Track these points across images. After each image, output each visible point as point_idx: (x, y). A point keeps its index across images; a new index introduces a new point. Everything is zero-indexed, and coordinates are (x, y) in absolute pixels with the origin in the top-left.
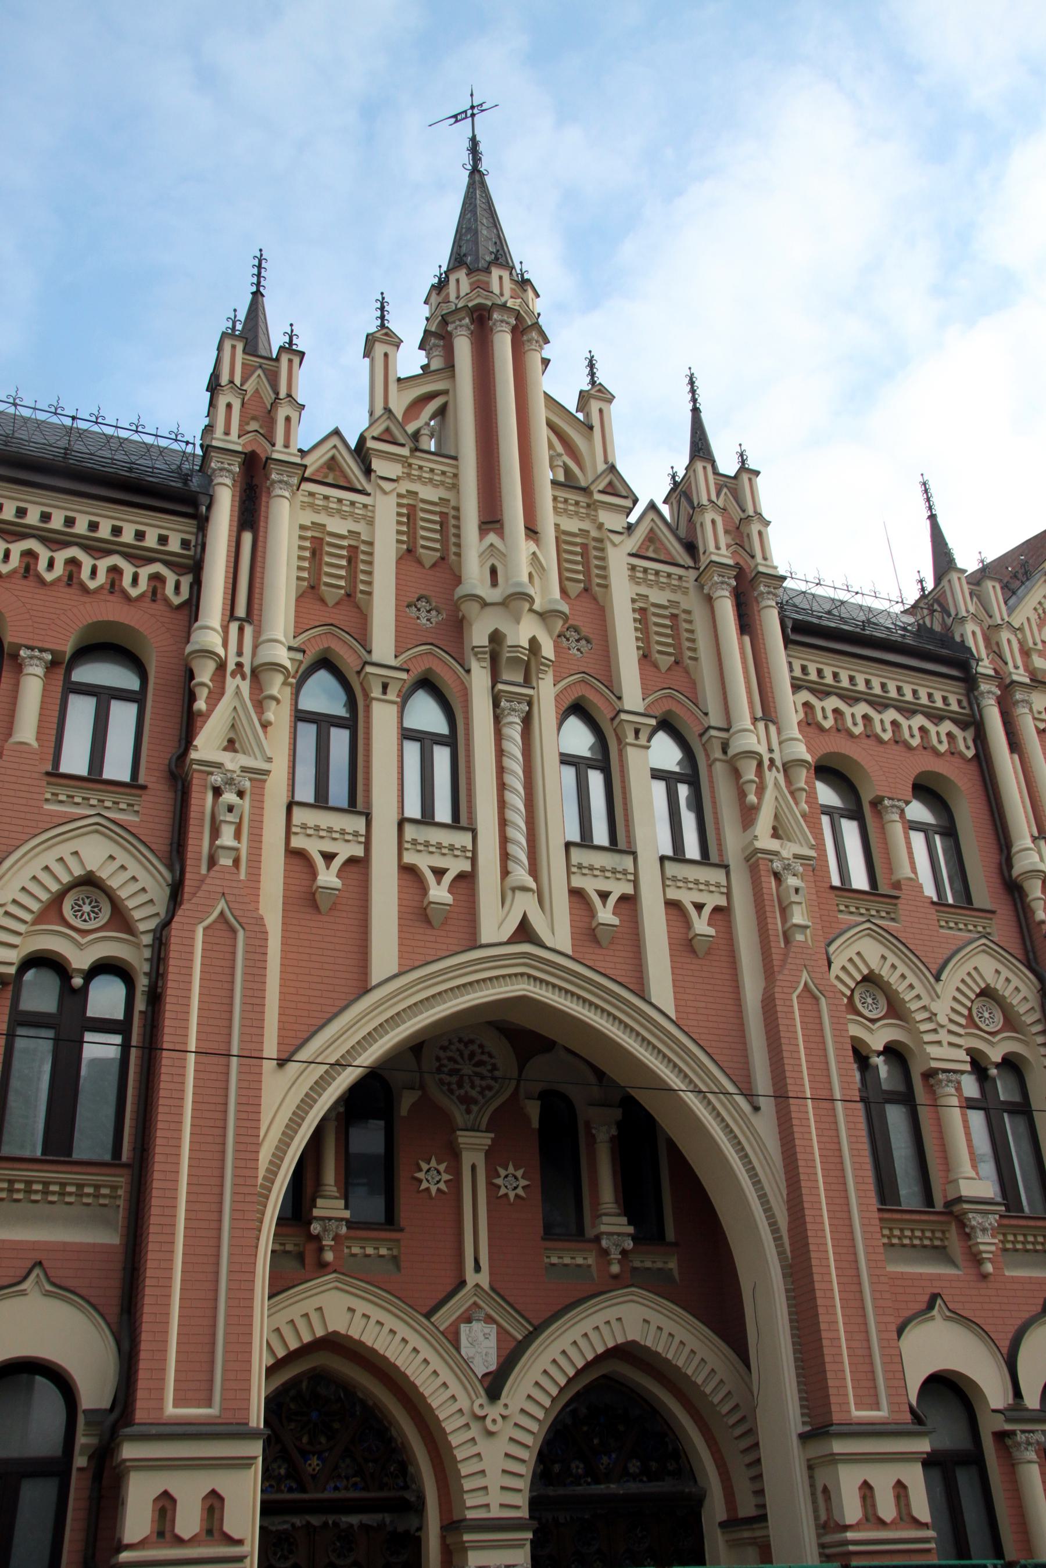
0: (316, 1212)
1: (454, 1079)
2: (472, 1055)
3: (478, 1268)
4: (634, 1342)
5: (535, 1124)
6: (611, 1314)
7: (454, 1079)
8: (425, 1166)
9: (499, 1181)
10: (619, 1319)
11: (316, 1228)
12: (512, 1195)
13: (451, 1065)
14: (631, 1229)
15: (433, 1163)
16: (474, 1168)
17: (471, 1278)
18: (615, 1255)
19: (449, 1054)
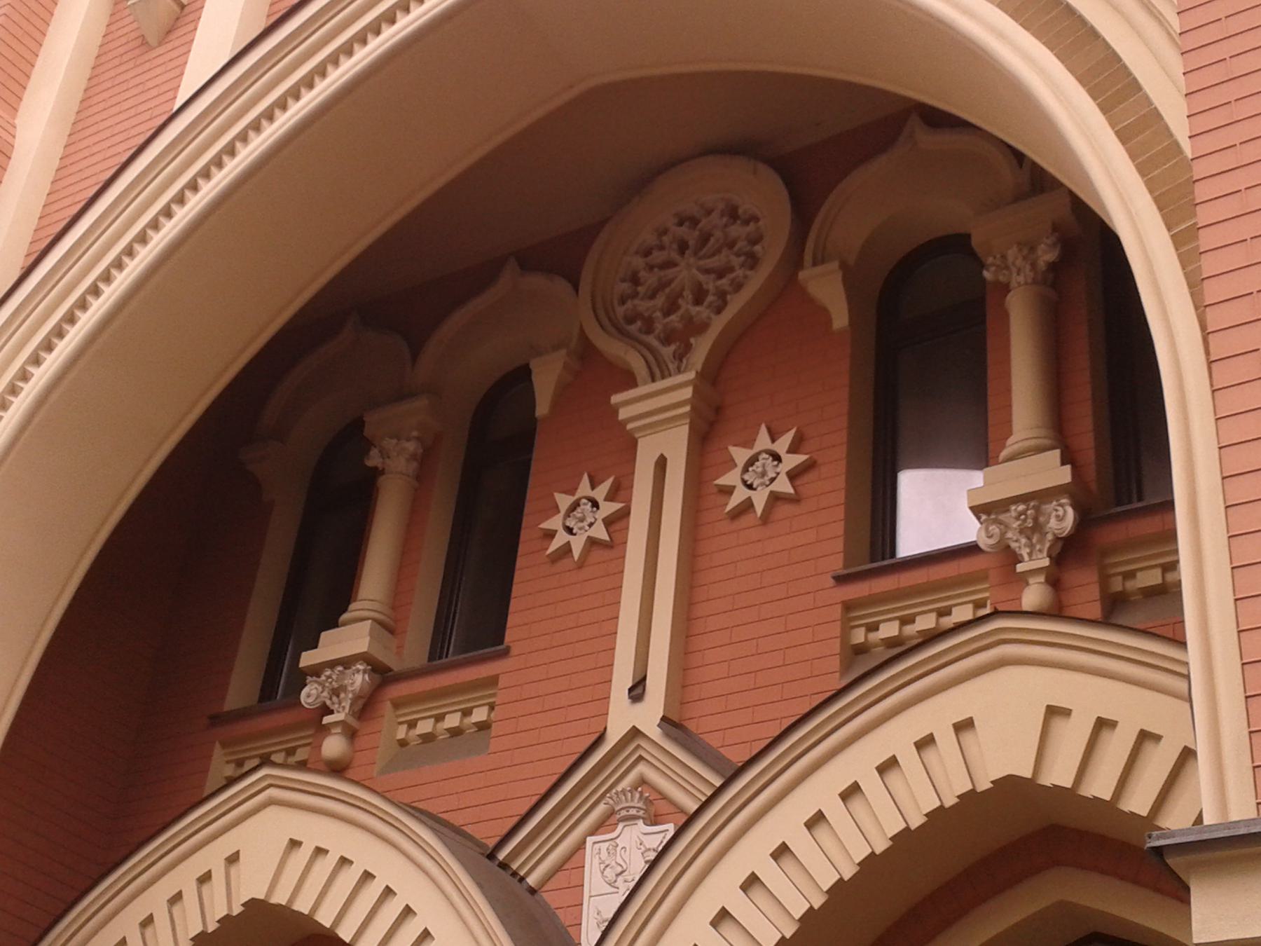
0: (308, 659)
1: (660, 300)
2: (705, 238)
3: (637, 691)
4: (1008, 785)
5: (840, 319)
6: (935, 716)
7: (660, 300)
8: (564, 501)
9: (731, 478)
10: (964, 726)
11: (310, 695)
12: (760, 500)
13: (651, 279)
14: (1064, 475)
15: (584, 488)
16: (661, 464)
17: (621, 717)
18: (1035, 560)
19: (658, 257)
